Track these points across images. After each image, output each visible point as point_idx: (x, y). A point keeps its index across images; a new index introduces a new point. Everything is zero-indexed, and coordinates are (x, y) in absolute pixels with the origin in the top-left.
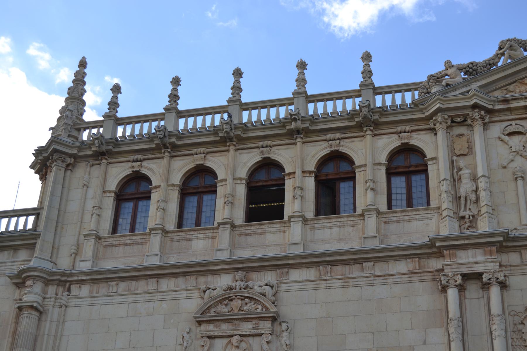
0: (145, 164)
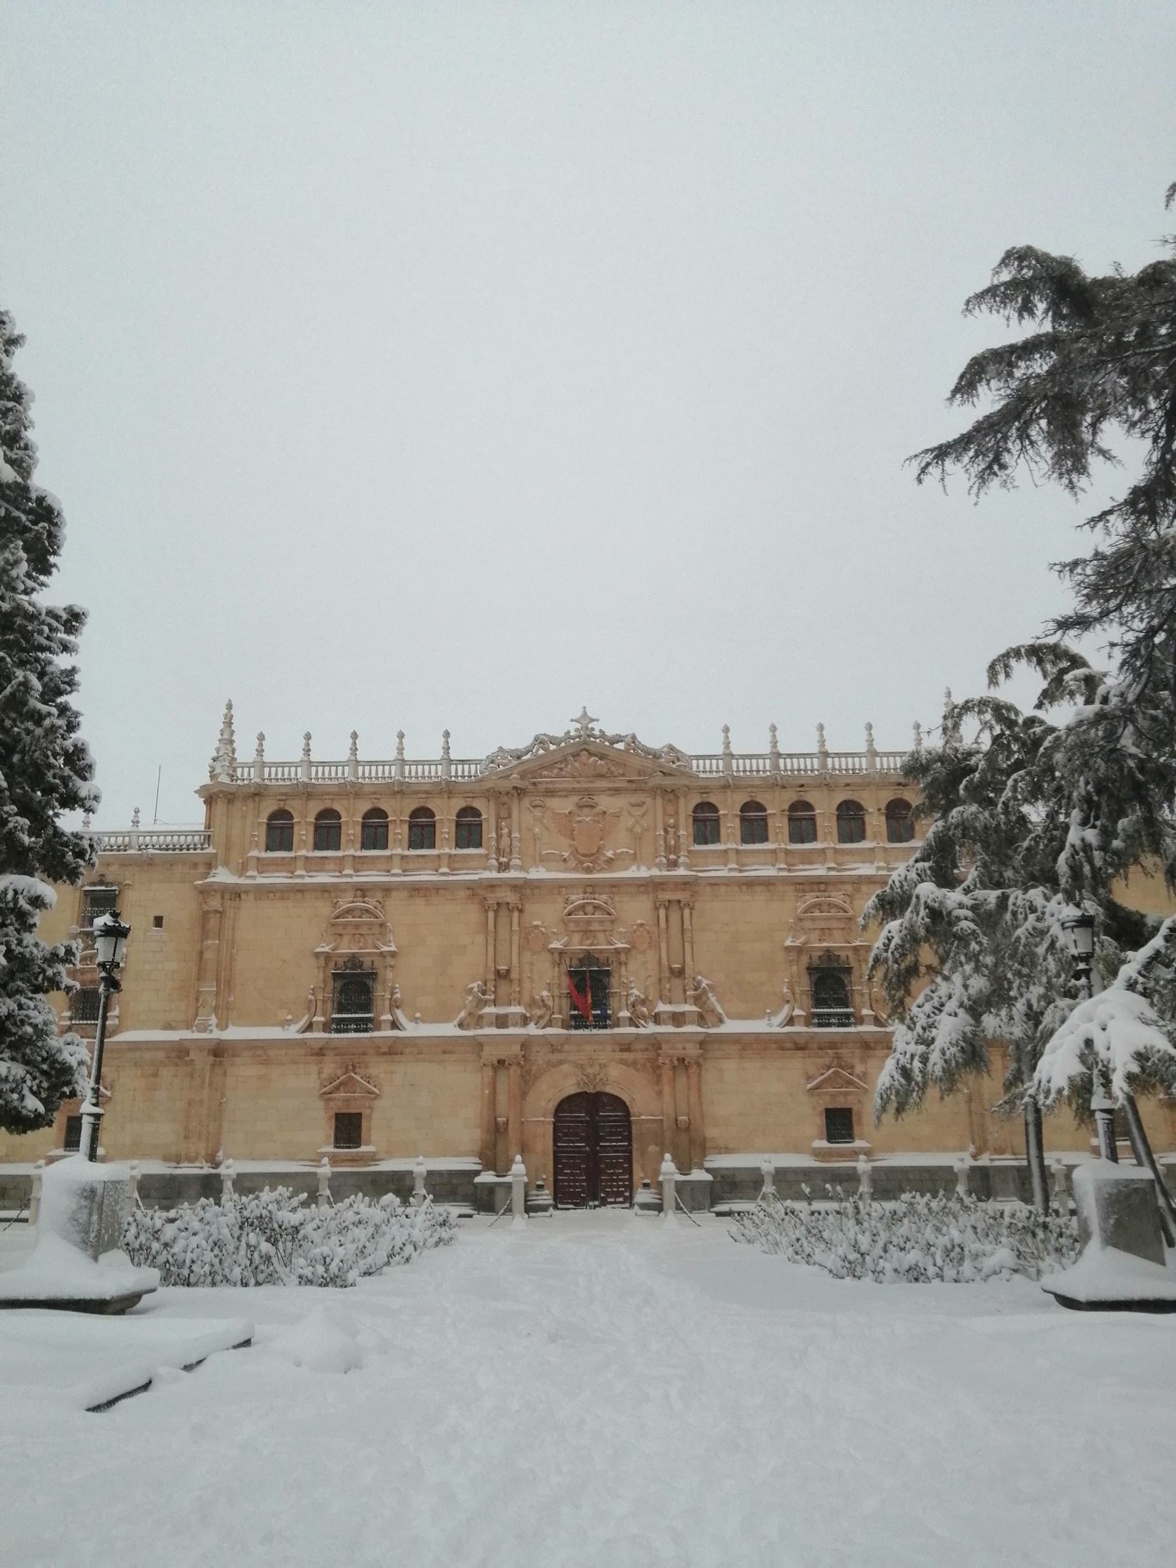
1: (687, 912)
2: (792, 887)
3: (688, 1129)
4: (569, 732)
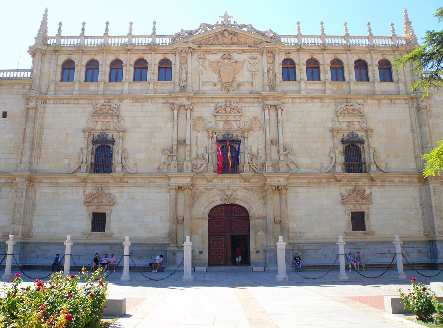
0: (72, 56)
1: (280, 111)
2: (333, 101)
3: (280, 222)
4: (218, 22)
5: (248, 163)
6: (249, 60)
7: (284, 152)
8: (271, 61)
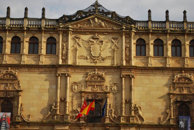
5: (109, 116)
6: (112, 40)
7: (134, 108)
8: (128, 41)
